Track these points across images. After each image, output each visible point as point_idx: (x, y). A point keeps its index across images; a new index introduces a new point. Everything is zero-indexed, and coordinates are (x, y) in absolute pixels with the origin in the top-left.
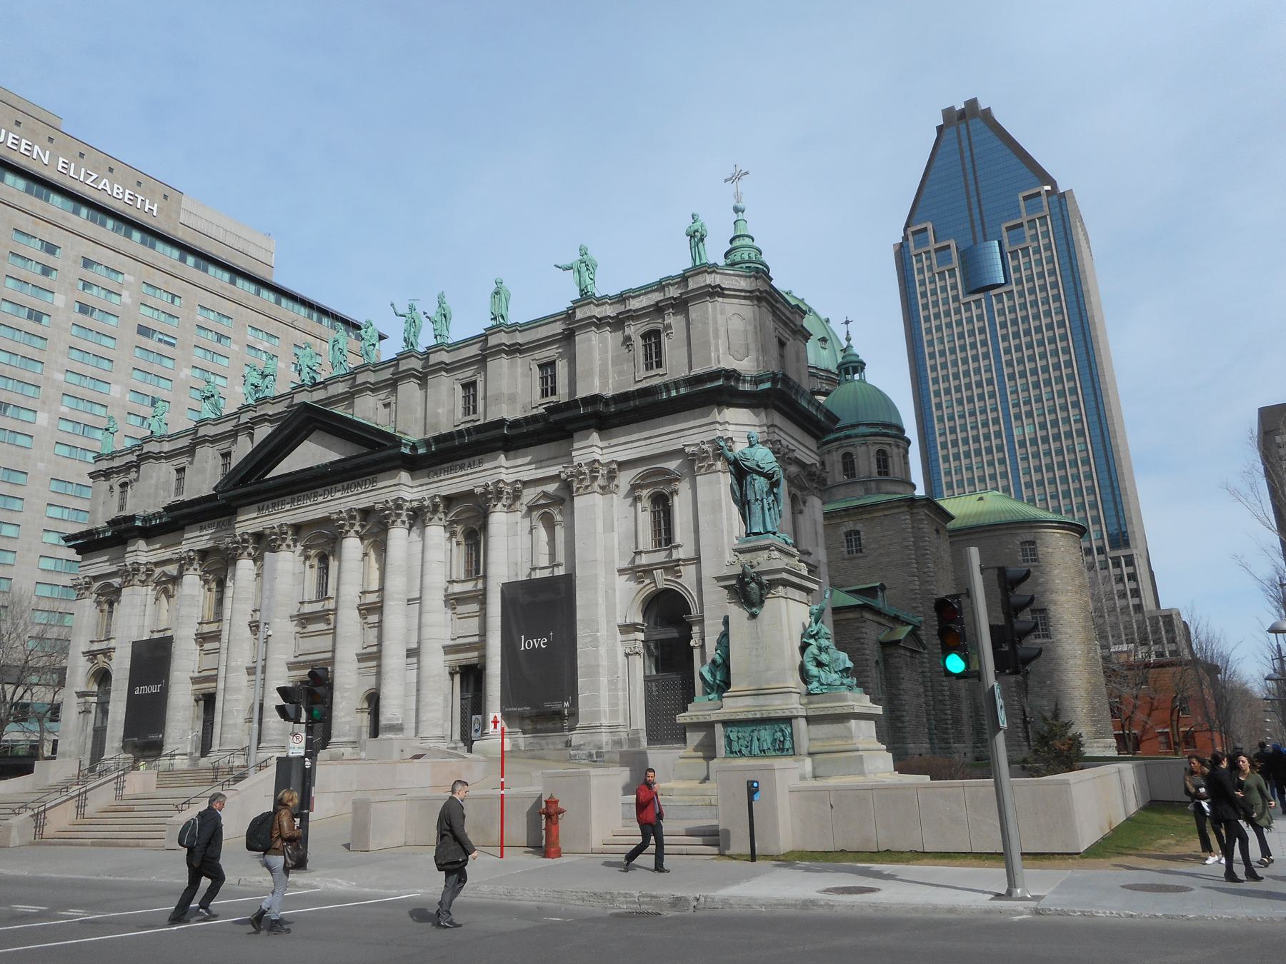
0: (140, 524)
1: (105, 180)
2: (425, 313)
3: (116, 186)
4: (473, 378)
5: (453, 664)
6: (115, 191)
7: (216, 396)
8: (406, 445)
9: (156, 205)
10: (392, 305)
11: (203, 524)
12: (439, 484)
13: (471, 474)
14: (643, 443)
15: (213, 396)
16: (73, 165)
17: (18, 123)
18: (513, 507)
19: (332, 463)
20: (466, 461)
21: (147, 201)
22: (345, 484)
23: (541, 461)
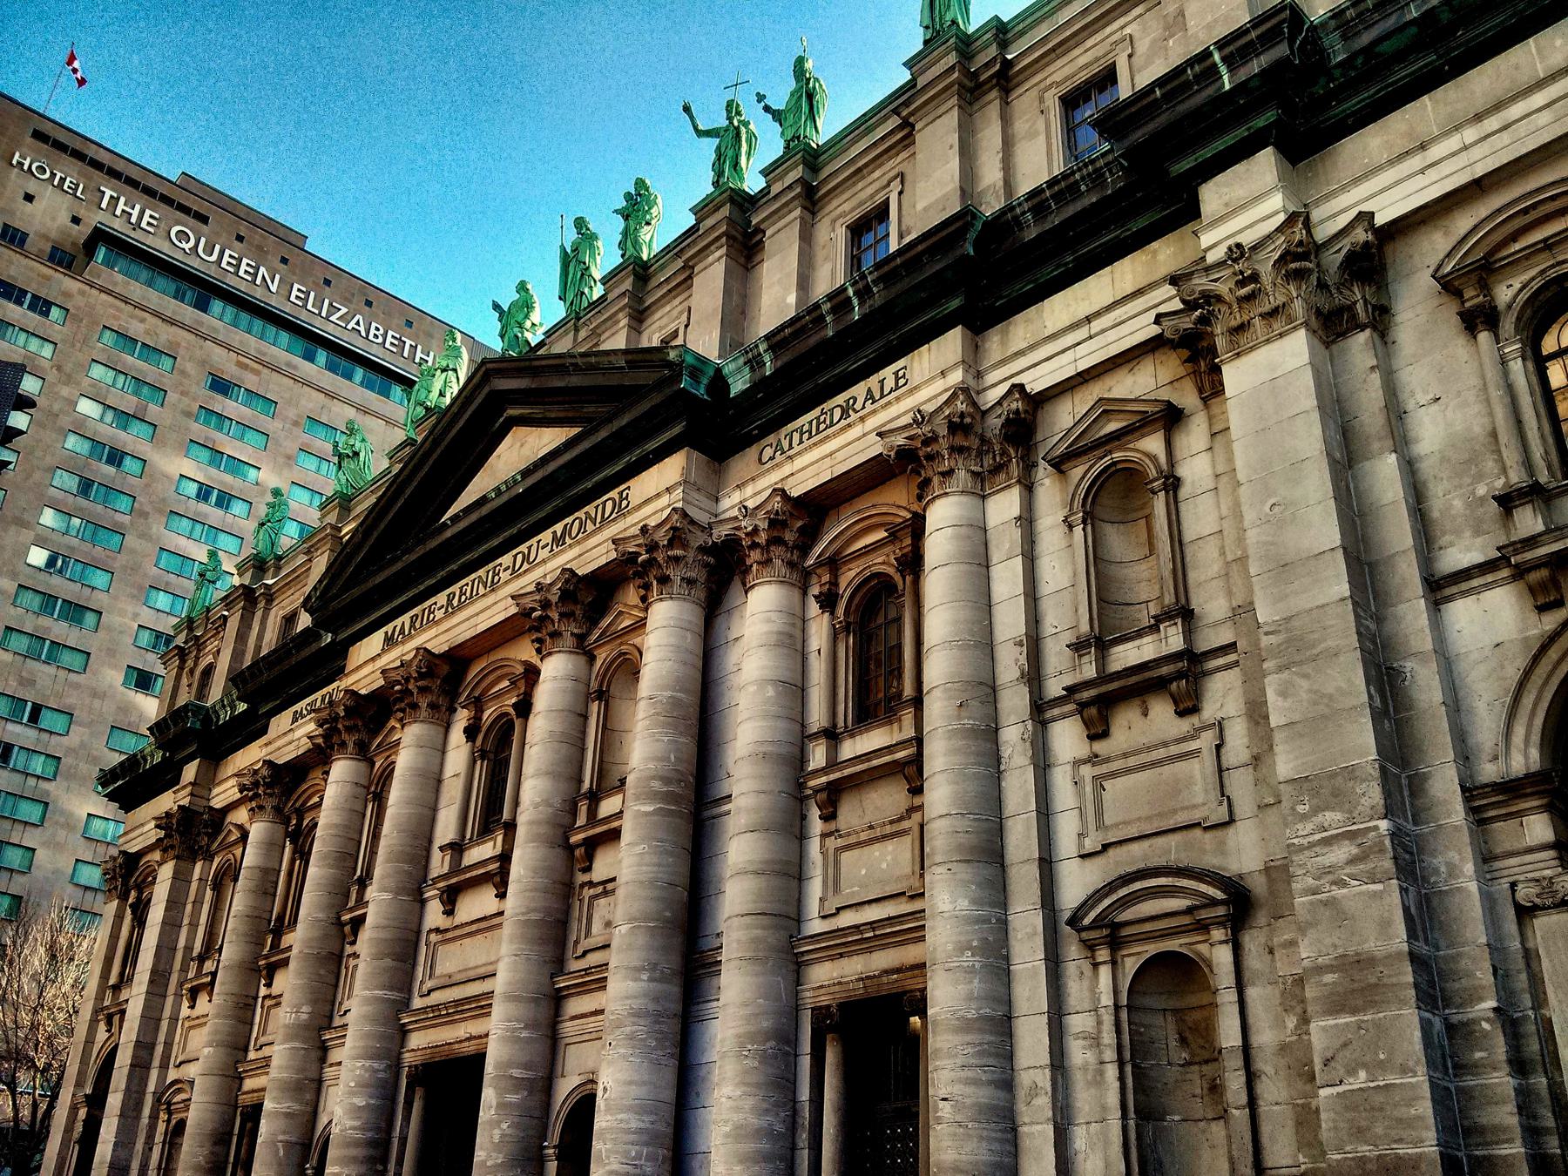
0: (198, 726)
1: (358, 317)
2: (761, 98)
3: (374, 325)
4: (879, 199)
5: (825, 1000)
6: (373, 331)
7: (362, 455)
8: (695, 373)
9: (432, 354)
10: (687, 109)
11: (297, 707)
12: (787, 469)
13: (874, 412)
14: (1470, 134)
15: (356, 454)
16: (312, 294)
17: (240, 238)
18: (1003, 476)
19: (526, 473)
20: (859, 390)
21: (419, 348)
22: (559, 527)
23: (1088, 319)
